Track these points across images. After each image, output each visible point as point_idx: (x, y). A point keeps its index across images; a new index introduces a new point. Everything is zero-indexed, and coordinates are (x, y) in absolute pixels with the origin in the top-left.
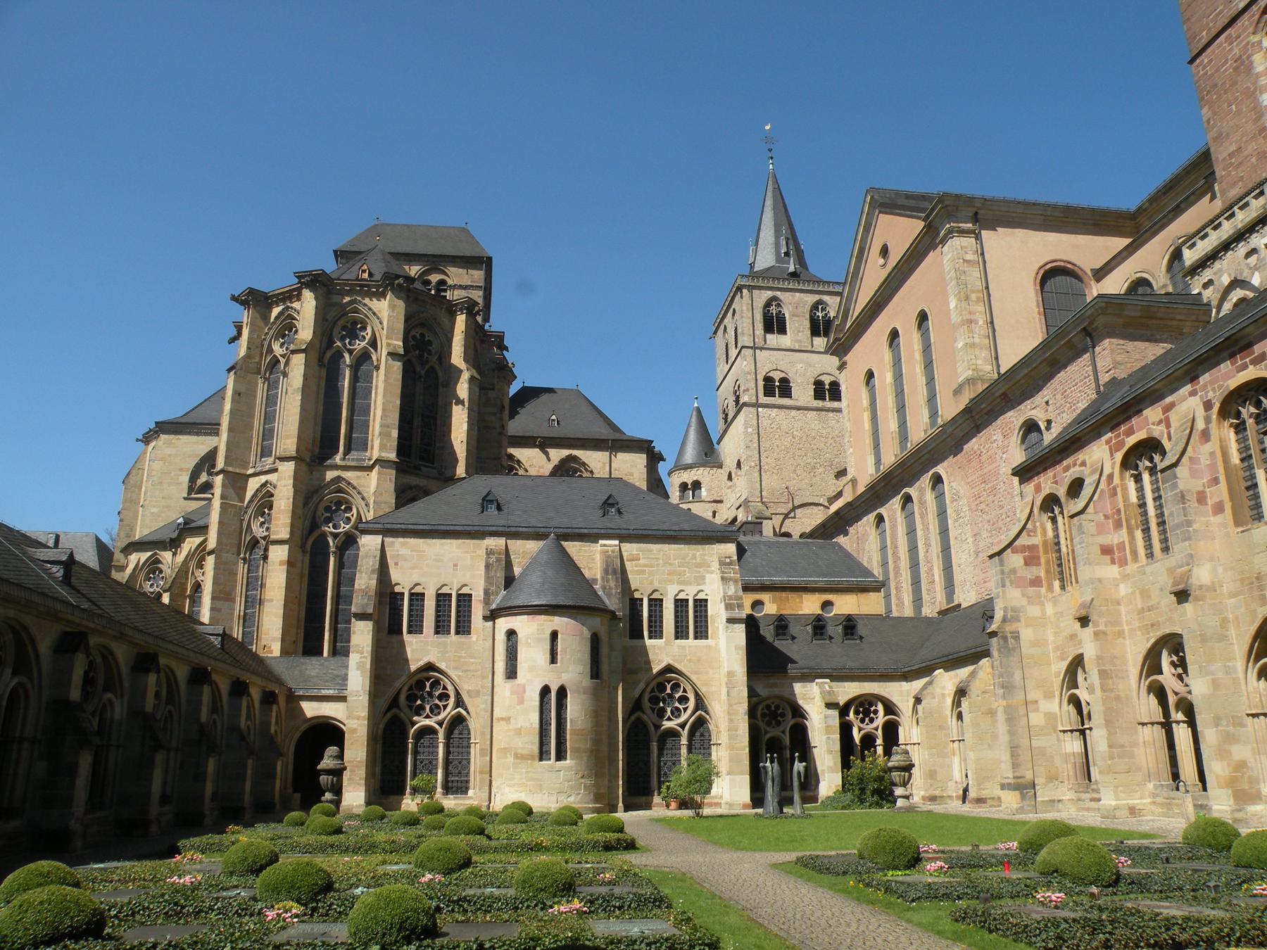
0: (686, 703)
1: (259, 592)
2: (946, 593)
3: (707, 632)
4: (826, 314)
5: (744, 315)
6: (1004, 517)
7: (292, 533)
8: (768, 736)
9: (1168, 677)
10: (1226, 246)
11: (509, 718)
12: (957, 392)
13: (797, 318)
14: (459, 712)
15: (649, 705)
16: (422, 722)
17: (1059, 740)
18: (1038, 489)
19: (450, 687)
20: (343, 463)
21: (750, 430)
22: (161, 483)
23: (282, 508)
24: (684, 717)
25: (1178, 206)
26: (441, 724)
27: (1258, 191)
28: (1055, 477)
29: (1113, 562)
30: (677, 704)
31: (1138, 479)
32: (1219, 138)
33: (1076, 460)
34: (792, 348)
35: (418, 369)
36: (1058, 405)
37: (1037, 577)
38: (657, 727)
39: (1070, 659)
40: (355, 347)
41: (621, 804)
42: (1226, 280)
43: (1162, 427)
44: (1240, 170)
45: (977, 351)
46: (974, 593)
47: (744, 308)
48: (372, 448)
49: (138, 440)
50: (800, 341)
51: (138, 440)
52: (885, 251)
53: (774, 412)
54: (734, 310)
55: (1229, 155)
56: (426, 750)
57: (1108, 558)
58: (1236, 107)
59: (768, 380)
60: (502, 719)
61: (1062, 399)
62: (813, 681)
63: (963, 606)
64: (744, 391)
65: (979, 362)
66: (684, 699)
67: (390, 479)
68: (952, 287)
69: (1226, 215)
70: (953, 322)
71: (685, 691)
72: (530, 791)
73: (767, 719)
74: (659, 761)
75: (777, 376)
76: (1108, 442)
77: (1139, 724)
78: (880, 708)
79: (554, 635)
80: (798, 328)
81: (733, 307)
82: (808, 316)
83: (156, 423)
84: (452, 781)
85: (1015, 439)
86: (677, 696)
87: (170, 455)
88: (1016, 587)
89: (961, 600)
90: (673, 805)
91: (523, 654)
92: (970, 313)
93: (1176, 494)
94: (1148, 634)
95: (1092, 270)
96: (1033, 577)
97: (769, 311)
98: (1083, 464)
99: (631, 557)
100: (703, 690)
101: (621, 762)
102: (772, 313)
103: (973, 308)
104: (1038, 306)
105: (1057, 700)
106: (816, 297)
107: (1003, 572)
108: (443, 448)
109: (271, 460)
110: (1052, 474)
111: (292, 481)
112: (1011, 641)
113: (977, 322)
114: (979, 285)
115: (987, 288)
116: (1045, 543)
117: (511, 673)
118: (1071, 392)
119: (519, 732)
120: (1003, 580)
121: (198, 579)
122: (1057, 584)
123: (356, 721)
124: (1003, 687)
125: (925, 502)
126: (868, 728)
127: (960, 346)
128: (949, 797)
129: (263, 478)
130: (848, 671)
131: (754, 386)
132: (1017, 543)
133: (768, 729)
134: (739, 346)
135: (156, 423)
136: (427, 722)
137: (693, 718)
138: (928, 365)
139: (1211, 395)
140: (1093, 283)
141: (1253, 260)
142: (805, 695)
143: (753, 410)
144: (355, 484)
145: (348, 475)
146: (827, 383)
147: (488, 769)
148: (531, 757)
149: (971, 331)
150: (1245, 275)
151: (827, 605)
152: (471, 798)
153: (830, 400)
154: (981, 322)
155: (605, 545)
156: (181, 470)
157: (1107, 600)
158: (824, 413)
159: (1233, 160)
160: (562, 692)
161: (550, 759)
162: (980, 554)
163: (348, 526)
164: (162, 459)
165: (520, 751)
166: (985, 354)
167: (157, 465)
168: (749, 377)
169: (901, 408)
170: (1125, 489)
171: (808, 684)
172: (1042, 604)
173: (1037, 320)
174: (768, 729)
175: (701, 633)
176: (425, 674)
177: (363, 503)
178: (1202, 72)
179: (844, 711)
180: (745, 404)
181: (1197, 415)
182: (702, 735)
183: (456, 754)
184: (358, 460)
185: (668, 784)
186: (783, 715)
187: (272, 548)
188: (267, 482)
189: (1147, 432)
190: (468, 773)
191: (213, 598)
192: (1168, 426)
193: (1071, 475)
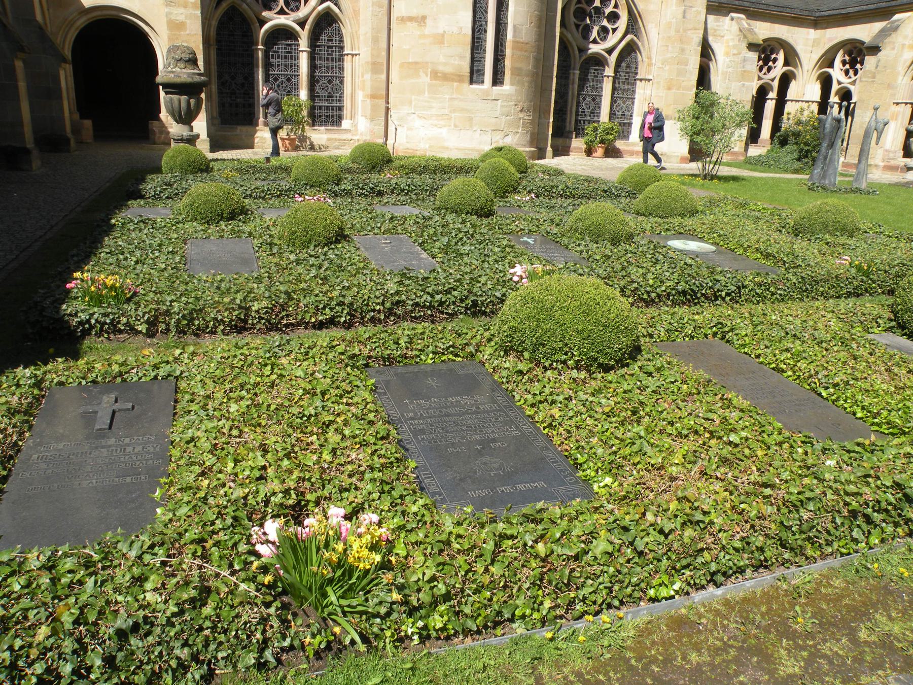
0: (615, 22)
11: (424, 18)
14: (328, 8)
16: (274, 20)
24: (612, 40)
26: (302, 24)
30: (605, 23)
38: (583, 50)
41: (549, 149)
56: (282, 61)
60: (411, 19)
62: (726, 15)
66: (614, 17)
72: (455, 126)
74: (579, 95)
78: (781, 57)
84: (320, 107)
90: (600, 151)
100: (641, 6)
101: (553, 93)
119: (440, 39)
123: (182, 10)
128: (876, 166)
130: (764, 7)
136: (282, 20)
142: (716, 30)
147: (384, 93)
148: (460, 79)
152: (347, 131)
161: (483, 82)
165: (441, 68)
171: (722, 18)
182: (628, 67)
183: (324, 69)
185: (596, 125)
190: (341, 97)
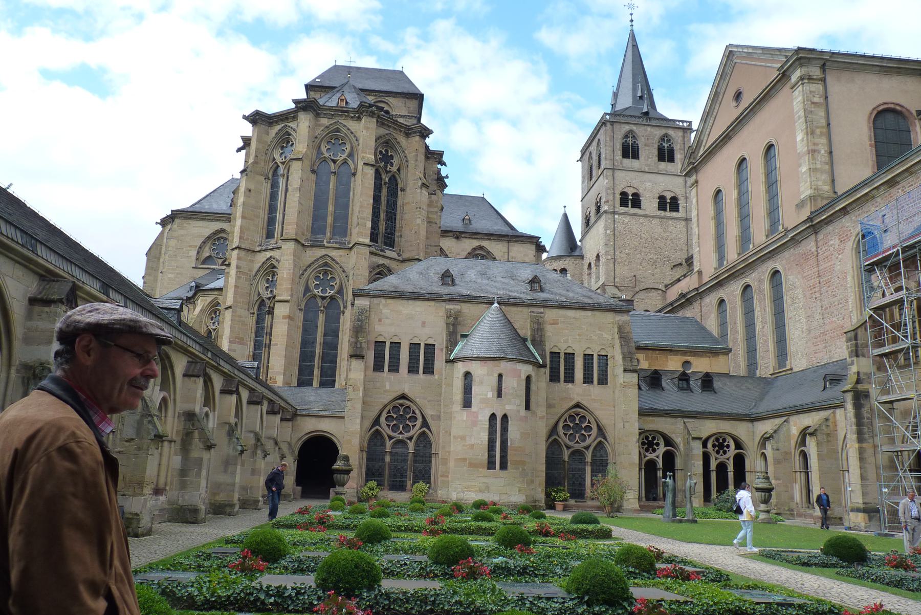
0: (590, 431)
1: (265, 338)
2: (778, 360)
3: (607, 379)
4: (670, 145)
5: (607, 144)
6: (836, 303)
7: (292, 296)
8: (647, 458)
12: (800, 205)
13: (647, 148)
15: (563, 431)
19: (417, 412)
20: (330, 245)
21: (608, 232)
22: (176, 256)
23: (285, 276)
24: (588, 441)
30: (583, 432)
34: (643, 170)
35: (383, 177)
40: (337, 158)
45: (819, 175)
46: (805, 361)
47: (608, 139)
48: (351, 235)
49: (157, 223)
50: (648, 165)
51: (157, 223)
52: (738, 96)
53: (627, 219)
54: (599, 140)
59: (624, 195)
63: (794, 371)
64: (605, 202)
65: (820, 183)
66: (588, 428)
67: (365, 258)
68: (800, 125)
70: (798, 151)
71: (589, 422)
73: (646, 446)
75: (630, 191)
79: (500, 376)
80: (648, 154)
81: (598, 137)
82: (656, 146)
83: (172, 211)
85: (850, 244)
86: (583, 426)
87: (182, 236)
89: (793, 366)
91: (475, 389)
92: (814, 144)
95: (916, 111)
97: (626, 141)
99: (552, 322)
100: (604, 421)
102: (629, 144)
103: (817, 140)
104: (870, 140)
106: (663, 131)
108: (401, 236)
109: (273, 241)
111: (292, 257)
113: (819, 152)
114: (823, 122)
115: (829, 125)
117: (467, 404)
119: (472, 446)
121: (209, 327)
125: (764, 290)
126: (722, 458)
127: (804, 170)
129: (268, 254)
131: (612, 198)
133: (647, 454)
134: (602, 167)
135: (172, 211)
136: (401, 437)
137: (596, 442)
138: (771, 185)
140: (917, 122)
143: (610, 216)
144: (338, 261)
145: (334, 253)
146: (668, 197)
149: (814, 159)
151: (687, 363)
153: (670, 211)
154: (823, 152)
155: (533, 312)
156: (190, 246)
158: (665, 220)
160: (505, 417)
162: (812, 332)
163: (332, 292)
164: (177, 238)
166: (825, 177)
167: (173, 243)
168: (609, 192)
169: (744, 217)
174: (647, 454)
175: (603, 381)
176: (401, 401)
177: (344, 275)
179: (705, 445)
180: (605, 212)
184: (340, 243)
186: (658, 444)
187: (276, 305)
188: (271, 257)
191: (230, 342)
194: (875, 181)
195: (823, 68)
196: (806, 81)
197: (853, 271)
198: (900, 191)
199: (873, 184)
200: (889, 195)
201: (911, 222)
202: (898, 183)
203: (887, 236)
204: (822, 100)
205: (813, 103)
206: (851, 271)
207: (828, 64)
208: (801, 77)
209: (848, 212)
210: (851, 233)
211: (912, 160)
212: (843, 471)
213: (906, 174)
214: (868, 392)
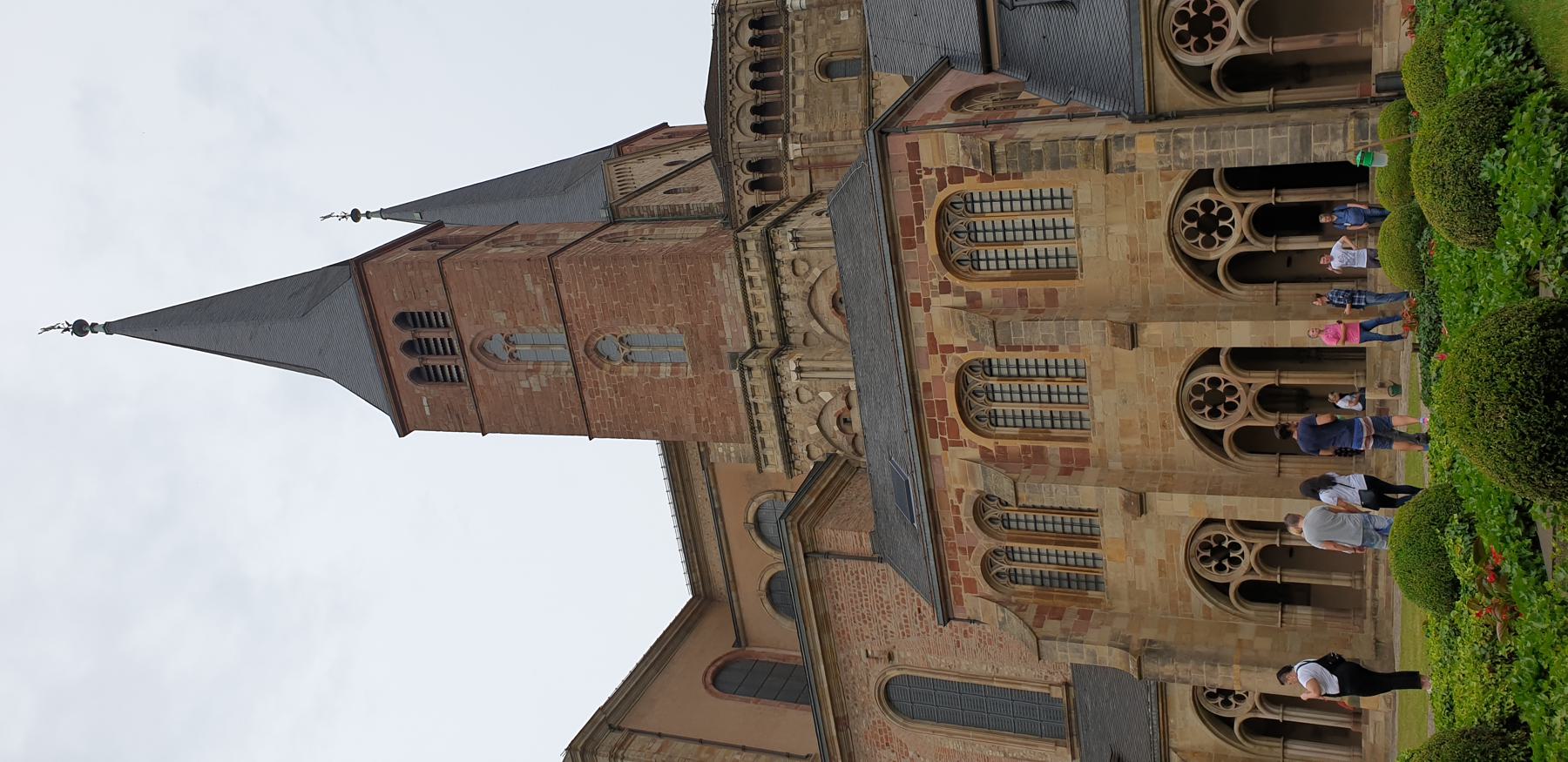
9: (1228, 425)
10: (781, 419)
17: (1295, 630)
18: (971, 586)
25: (714, 510)
27: (746, 373)
28: (963, 550)
29: (1083, 470)
31: (993, 418)
32: (674, 427)
33: (953, 506)
36: (875, 634)
37: (1078, 613)
39: (1189, 582)
42: (814, 430)
43: (950, 357)
44: (715, 415)
55: (696, 422)
57: (1074, 472)
58: (657, 403)
61: (870, 625)
69: (753, 411)
76: (945, 449)
77: (1279, 476)
85: (897, 728)
88: (1086, 631)
93: (1025, 327)
94: (1172, 435)
96: (1078, 616)
98: (960, 493)
104: (748, 701)
105: (1240, 622)
107: (1064, 640)
110: (959, 554)
112: (1154, 647)
114: (693, 747)
115: (701, 741)
116: (1037, 595)
118: (867, 606)
120: (1071, 641)
122: (1092, 594)
124: (1216, 666)
132: (1030, 623)
139: (935, 282)
140: (747, 649)
141: (806, 395)
150: (816, 406)
154: (738, 757)
157: (1124, 479)
159: (703, 419)
170: (1002, 437)
172: (1115, 615)
173: (762, 706)
178: (607, 429)
181: (950, 304)
189: (950, 381)
192: (949, 348)
193: (968, 520)
194: (812, 648)
195: (611, 727)
196: (622, 752)
197: (940, 732)
198: (839, 615)
199: (816, 653)
200: (839, 636)
201: (888, 608)
202: (826, 614)
203: (899, 655)
204: (660, 741)
205: (658, 752)
206: (938, 737)
207: (611, 721)
208: (611, 756)
209: (844, 718)
210: (879, 722)
211: (802, 579)
212: (1284, 757)
213: (818, 595)
214: (1145, 640)
